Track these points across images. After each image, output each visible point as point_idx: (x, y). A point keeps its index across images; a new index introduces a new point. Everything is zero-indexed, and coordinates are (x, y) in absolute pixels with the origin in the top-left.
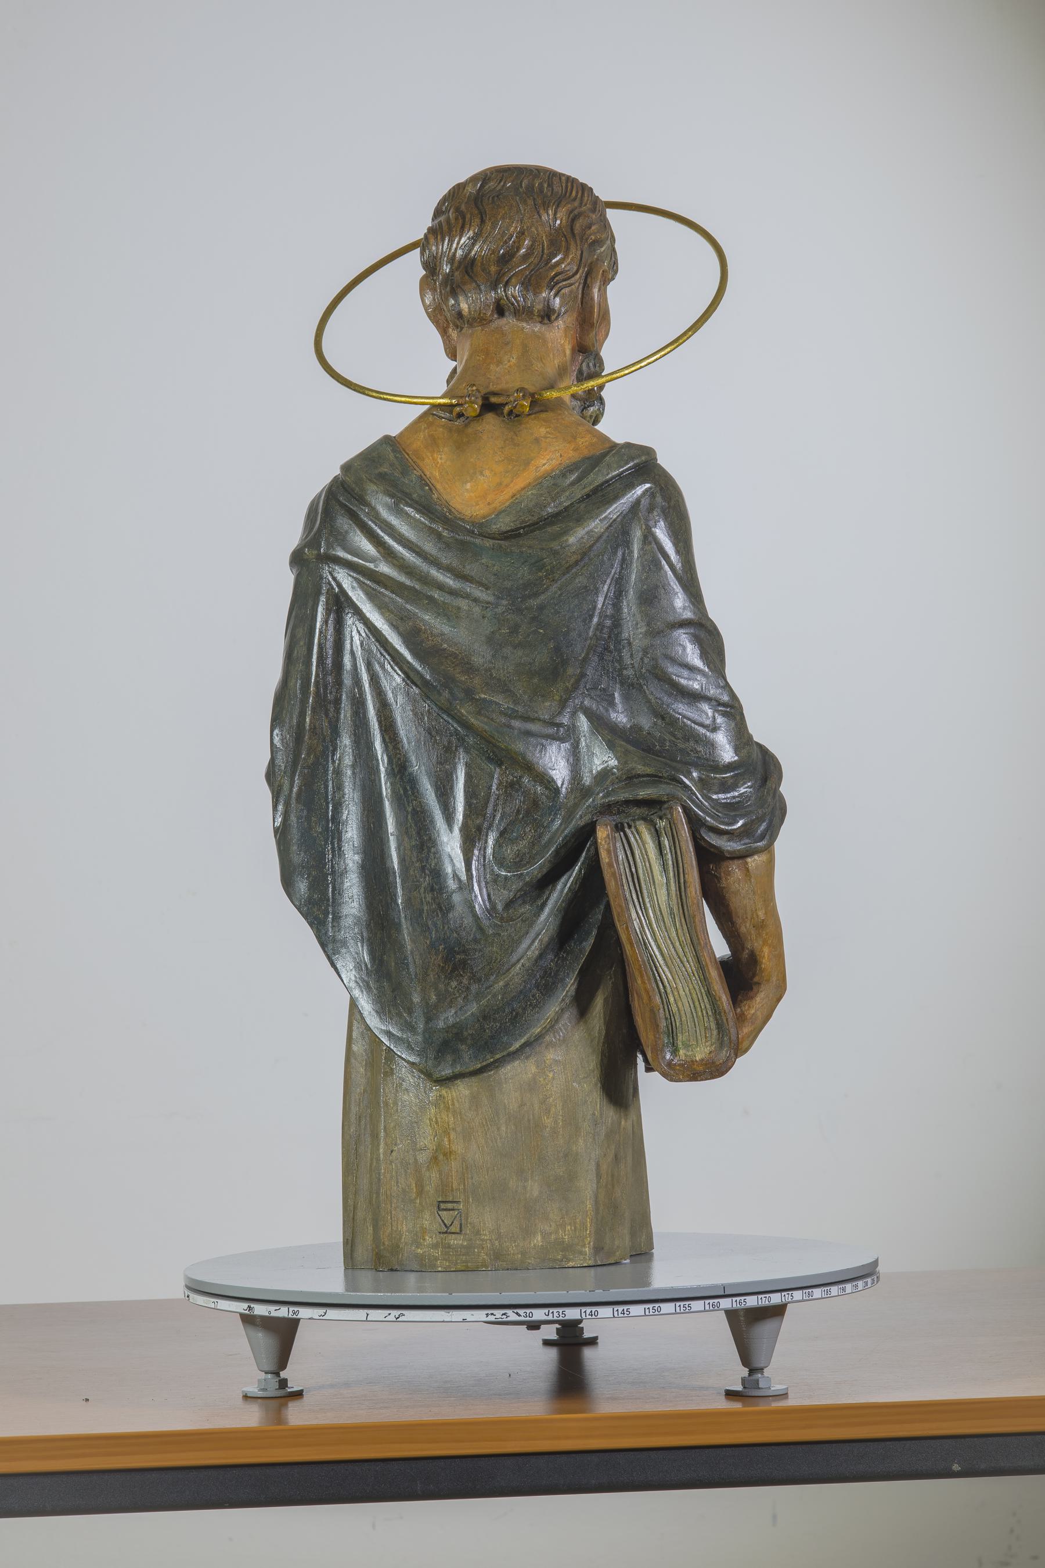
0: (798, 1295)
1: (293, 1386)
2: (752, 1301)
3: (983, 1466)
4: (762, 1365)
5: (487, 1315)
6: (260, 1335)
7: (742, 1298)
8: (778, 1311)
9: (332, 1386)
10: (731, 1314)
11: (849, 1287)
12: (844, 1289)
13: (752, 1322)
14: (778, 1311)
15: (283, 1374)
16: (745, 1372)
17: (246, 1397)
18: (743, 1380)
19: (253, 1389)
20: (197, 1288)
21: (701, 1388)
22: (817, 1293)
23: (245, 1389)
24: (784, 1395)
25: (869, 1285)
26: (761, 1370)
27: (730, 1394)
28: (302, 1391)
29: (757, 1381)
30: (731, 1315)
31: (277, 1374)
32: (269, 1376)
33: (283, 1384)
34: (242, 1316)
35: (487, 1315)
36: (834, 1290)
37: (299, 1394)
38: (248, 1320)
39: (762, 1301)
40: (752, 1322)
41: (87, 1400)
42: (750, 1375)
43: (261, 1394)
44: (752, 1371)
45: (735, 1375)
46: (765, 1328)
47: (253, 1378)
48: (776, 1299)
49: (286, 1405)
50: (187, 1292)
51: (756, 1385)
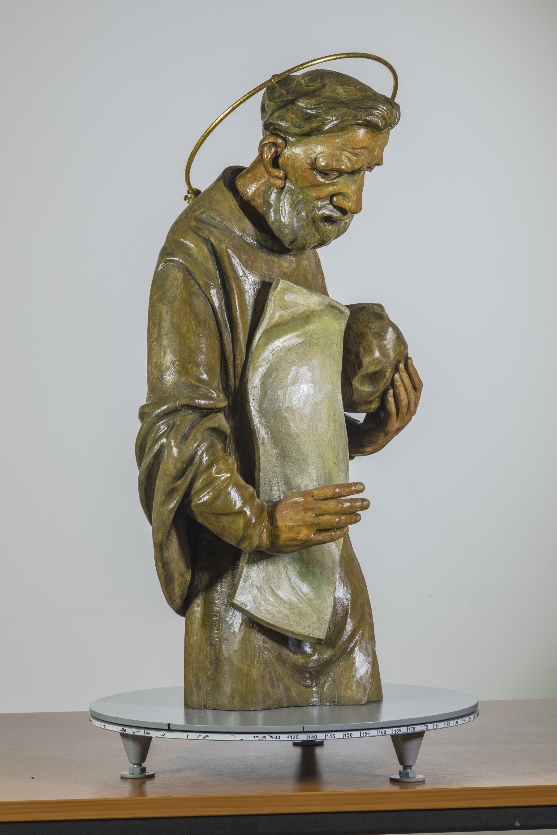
0: (430, 726)
1: (149, 772)
2: (404, 730)
3: (533, 824)
4: (411, 764)
5: (254, 737)
6: (130, 743)
7: (399, 728)
8: (420, 735)
9: (171, 771)
10: (394, 737)
11: (460, 721)
12: (457, 722)
13: (405, 741)
14: (420, 735)
15: (143, 765)
16: (401, 768)
17: (122, 778)
18: (400, 774)
19: (126, 773)
20: (96, 717)
21: (377, 776)
22: (442, 725)
23: (122, 773)
24: (423, 782)
25: (472, 719)
26: (410, 767)
27: (393, 781)
28: (154, 774)
29: (408, 773)
30: (394, 737)
31: (140, 765)
32: (136, 766)
33: (143, 770)
34: (121, 734)
35: (254, 737)
36: (452, 723)
37: (152, 776)
38: (124, 735)
39: (410, 730)
40: (405, 741)
41: (33, 778)
42: (404, 770)
43: (130, 776)
44: (405, 768)
45: (394, 769)
46: (413, 744)
47: (127, 768)
48: (418, 729)
49: (144, 783)
50: (91, 718)
51: (407, 775)
